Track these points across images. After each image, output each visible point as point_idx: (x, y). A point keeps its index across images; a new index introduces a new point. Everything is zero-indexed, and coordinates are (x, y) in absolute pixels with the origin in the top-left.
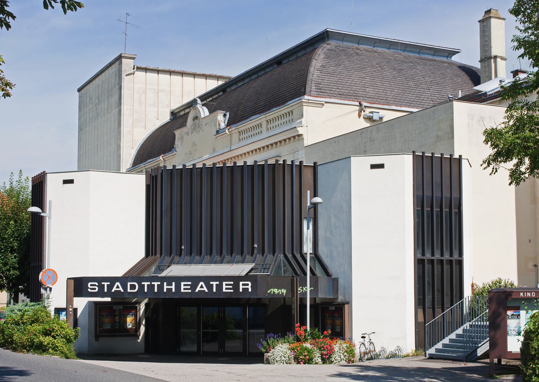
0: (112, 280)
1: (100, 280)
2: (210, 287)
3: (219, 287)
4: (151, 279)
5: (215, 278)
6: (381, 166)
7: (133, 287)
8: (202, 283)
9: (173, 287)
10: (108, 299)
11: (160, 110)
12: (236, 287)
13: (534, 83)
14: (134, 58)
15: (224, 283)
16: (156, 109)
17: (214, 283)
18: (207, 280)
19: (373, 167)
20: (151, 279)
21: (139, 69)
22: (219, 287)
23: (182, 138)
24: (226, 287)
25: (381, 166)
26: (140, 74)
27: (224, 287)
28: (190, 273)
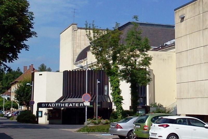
0: (51, 103)
1: (45, 103)
2: (73, 105)
3: (75, 105)
4: (61, 103)
5: (74, 103)
6: (41, 75)
7: (53, 105)
8: (71, 104)
9: (64, 105)
10: (52, 108)
11: (86, 42)
12: (79, 105)
13: (100, 37)
14: (76, 25)
15: (76, 104)
16: (84, 42)
17: (74, 104)
18: (72, 103)
19: (40, 75)
20: (63, 103)
21: (78, 28)
22: (75, 105)
23: (89, 54)
24: (77, 105)
25: (41, 75)
26: (79, 30)
27: (76, 105)
28: (72, 102)
